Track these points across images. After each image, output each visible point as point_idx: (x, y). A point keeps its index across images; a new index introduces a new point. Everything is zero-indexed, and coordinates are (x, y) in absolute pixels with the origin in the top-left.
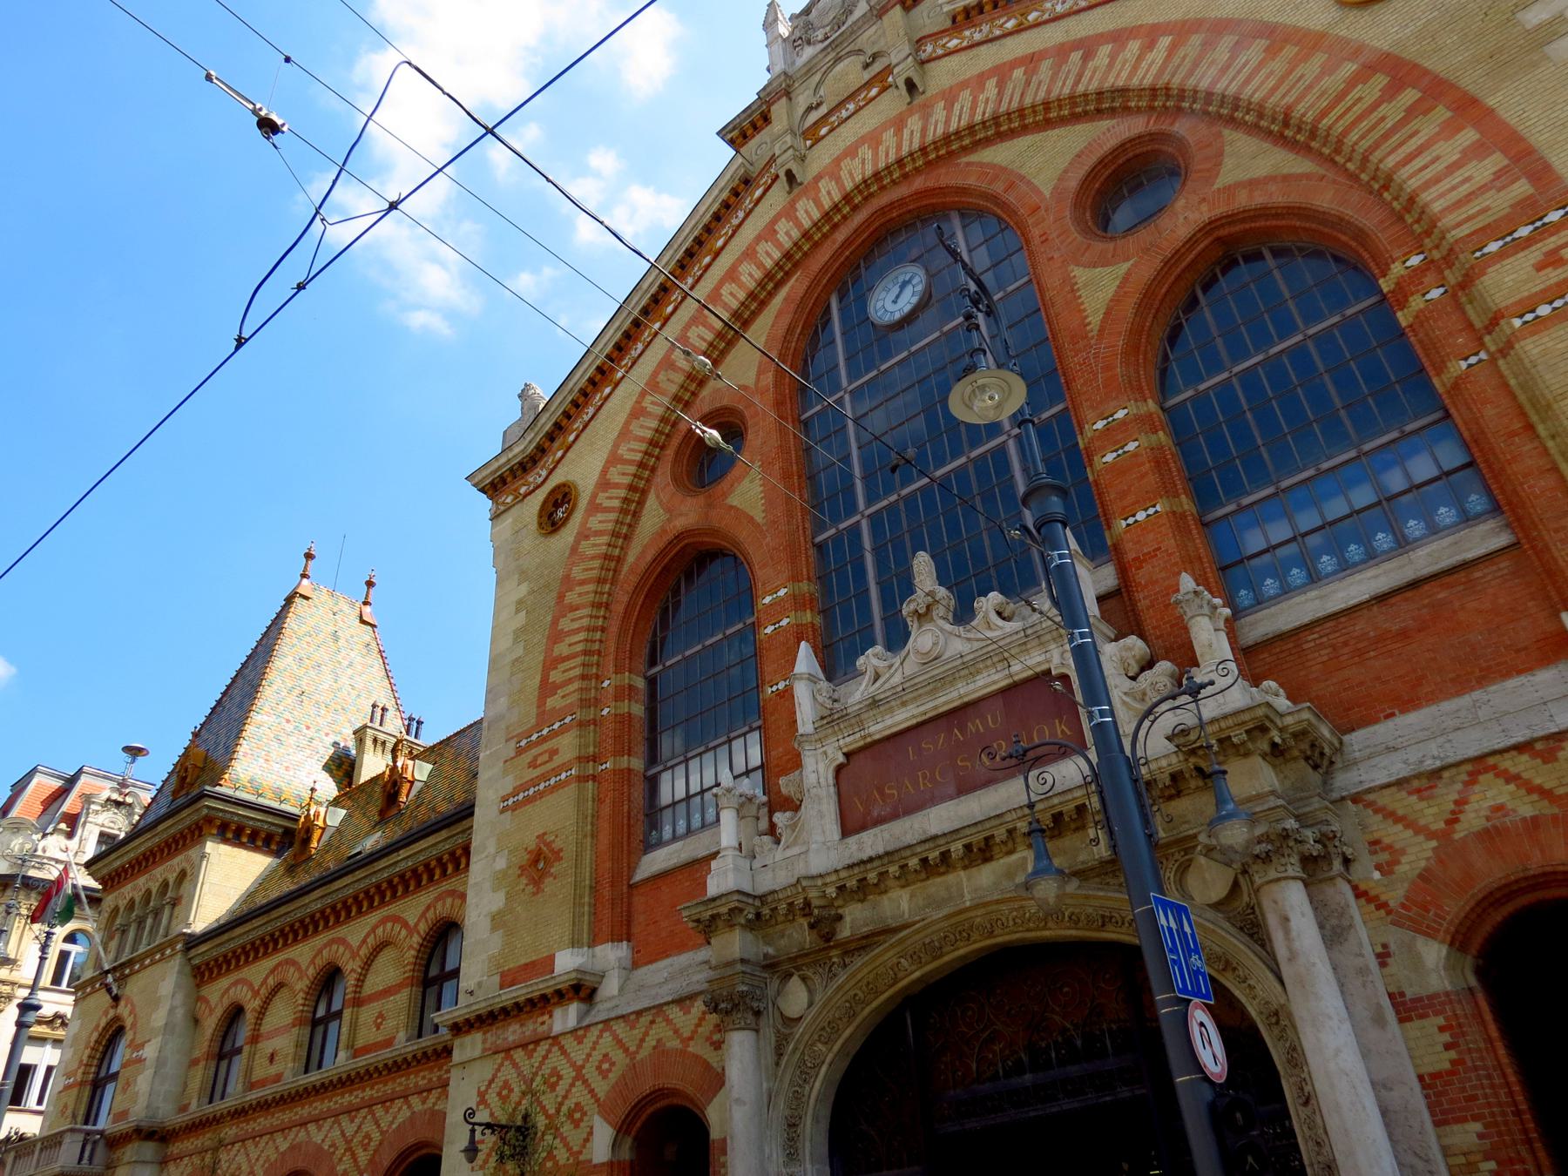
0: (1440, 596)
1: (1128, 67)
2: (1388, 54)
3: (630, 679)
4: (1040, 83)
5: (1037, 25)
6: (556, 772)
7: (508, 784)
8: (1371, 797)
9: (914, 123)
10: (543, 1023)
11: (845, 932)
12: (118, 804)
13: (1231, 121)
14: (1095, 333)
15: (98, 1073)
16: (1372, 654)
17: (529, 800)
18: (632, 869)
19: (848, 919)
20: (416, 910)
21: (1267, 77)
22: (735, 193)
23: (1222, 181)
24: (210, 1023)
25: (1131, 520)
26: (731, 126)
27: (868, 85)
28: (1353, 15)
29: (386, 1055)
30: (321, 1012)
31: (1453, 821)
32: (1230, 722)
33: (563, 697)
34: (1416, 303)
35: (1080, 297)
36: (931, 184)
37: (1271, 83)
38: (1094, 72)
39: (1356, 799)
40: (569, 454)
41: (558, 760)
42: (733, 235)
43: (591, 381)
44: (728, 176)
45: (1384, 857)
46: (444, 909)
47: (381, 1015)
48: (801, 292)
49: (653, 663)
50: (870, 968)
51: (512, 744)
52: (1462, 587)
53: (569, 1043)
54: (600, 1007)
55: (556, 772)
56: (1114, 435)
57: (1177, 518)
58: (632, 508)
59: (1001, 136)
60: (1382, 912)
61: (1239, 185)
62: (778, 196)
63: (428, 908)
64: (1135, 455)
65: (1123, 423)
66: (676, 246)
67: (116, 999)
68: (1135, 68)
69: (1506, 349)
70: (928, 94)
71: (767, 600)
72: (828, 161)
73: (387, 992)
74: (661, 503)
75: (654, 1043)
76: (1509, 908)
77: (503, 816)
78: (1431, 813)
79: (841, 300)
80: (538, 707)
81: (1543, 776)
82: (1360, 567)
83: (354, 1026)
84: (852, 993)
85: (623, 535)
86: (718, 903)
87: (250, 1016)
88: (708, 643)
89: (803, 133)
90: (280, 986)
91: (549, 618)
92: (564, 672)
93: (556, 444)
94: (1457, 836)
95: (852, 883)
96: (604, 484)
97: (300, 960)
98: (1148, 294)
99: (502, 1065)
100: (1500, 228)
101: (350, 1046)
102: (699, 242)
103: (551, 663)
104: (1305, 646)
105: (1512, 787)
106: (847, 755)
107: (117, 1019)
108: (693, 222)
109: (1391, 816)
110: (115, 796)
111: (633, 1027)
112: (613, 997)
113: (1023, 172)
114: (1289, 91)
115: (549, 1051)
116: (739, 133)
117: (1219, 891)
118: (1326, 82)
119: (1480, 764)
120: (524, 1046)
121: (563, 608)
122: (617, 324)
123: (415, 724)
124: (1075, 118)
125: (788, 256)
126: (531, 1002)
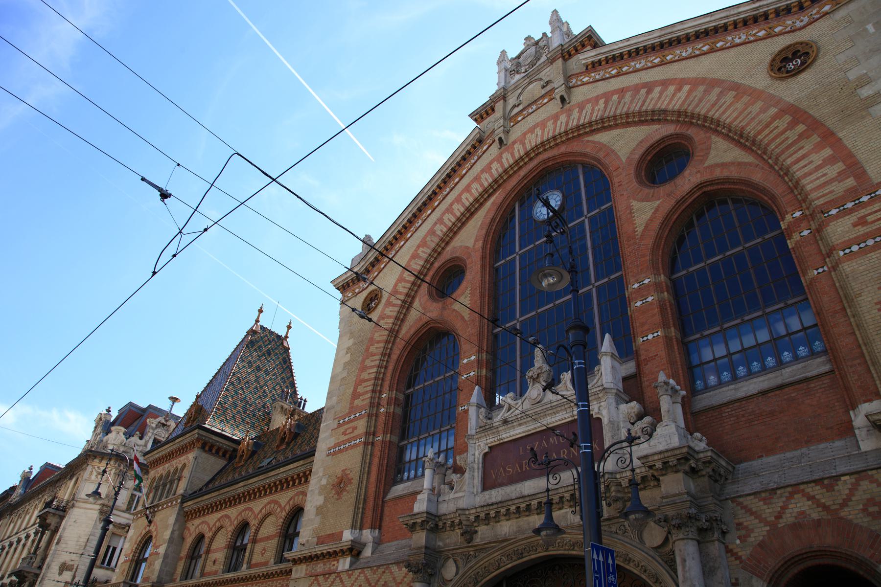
0: (793, 395)
1: (668, 99)
2: (793, 105)
3: (396, 394)
4: (625, 103)
5: (627, 73)
6: (355, 438)
7: (332, 442)
8: (741, 500)
9: (563, 118)
10: (334, 565)
11: (478, 540)
12: (164, 425)
13: (716, 132)
14: (639, 237)
15: (139, 557)
16: (756, 422)
17: (340, 451)
18: (386, 493)
19: (479, 533)
20: (285, 499)
21: (734, 111)
22: (474, 147)
23: (710, 161)
24: (189, 540)
25: (645, 339)
26: (476, 112)
27: (543, 97)
28: (777, 83)
29: (263, 570)
30: (238, 544)
31: (779, 517)
32: (669, 454)
33: (362, 400)
34: (796, 237)
35: (634, 216)
36: (569, 149)
37: (735, 114)
38: (651, 100)
39: (733, 500)
40: (380, 274)
41: (356, 433)
42: (470, 168)
43: (395, 238)
44: (471, 138)
45: (743, 532)
46: (298, 500)
47: (264, 549)
48: (500, 201)
49: (409, 387)
50: (487, 559)
51: (336, 421)
52: (803, 392)
53: (344, 576)
54: (362, 561)
55: (355, 438)
56: (642, 292)
57: (667, 339)
58: (407, 305)
59: (604, 129)
60: (738, 562)
61: (717, 165)
62: (494, 150)
63: (291, 499)
64: (651, 303)
65: (648, 285)
66: (442, 172)
67: (150, 522)
68: (671, 100)
69: (834, 268)
70: (572, 103)
71: (465, 361)
72: (520, 134)
73: (268, 538)
74: (421, 304)
75: (383, 583)
76: (802, 567)
77: (328, 458)
78: (768, 512)
79: (520, 206)
80: (350, 404)
81: (826, 499)
82: (756, 375)
83: (252, 553)
84: (476, 571)
85: (400, 319)
86: (417, 517)
87: (207, 540)
88: (436, 380)
89: (510, 118)
90: (221, 528)
91: (361, 359)
92: (365, 387)
93: (375, 268)
94: (780, 526)
95: (482, 515)
96: (394, 293)
97: (231, 516)
98: (667, 218)
99: (313, 583)
100: (837, 202)
101: (249, 562)
102: (454, 170)
103: (360, 382)
104: (724, 415)
105: (810, 503)
106: (490, 447)
107: (149, 532)
108: (452, 160)
109: (749, 511)
110: (163, 421)
111: (374, 574)
112: (369, 557)
113: (613, 148)
114: (743, 119)
115: (335, 579)
116: (479, 115)
117: (658, 541)
118: (762, 116)
119: (796, 488)
120: (324, 575)
121: (368, 354)
122: (410, 209)
123: (303, 402)
124: (641, 123)
125: (495, 181)
126: (329, 554)
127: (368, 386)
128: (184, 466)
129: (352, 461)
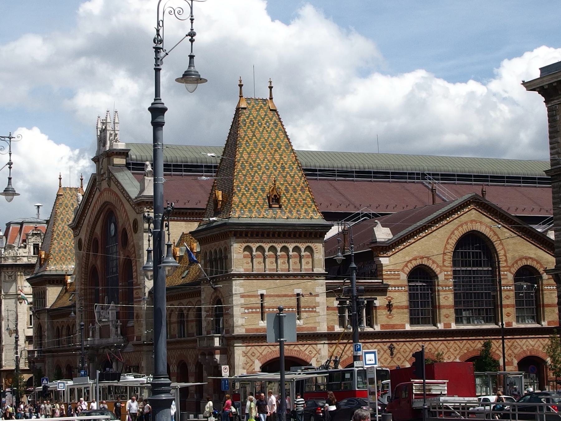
12: (36, 234)
24: (55, 329)
67: (39, 319)
87: (60, 331)
90: (63, 326)
96: (84, 245)
98: (124, 263)
107: (40, 323)
110: (34, 232)
121: (82, 273)
128: (44, 291)
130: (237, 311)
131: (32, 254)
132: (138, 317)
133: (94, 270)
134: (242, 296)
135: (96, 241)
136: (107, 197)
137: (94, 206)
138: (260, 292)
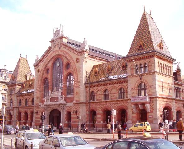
20: (31, 96)
23: (70, 69)
58: (43, 73)
85: (42, 75)
100: (76, 82)
103: (38, 84)
127: (39, 85)
129: (39, 95)
130: (157, 86)
131: (3, 79)
132: (77, 93)
133: (46, 78)
134: (158, 81)
135: (48, 69)
136: (57, 53)
137: (49, 57)
138: (162, 80)
